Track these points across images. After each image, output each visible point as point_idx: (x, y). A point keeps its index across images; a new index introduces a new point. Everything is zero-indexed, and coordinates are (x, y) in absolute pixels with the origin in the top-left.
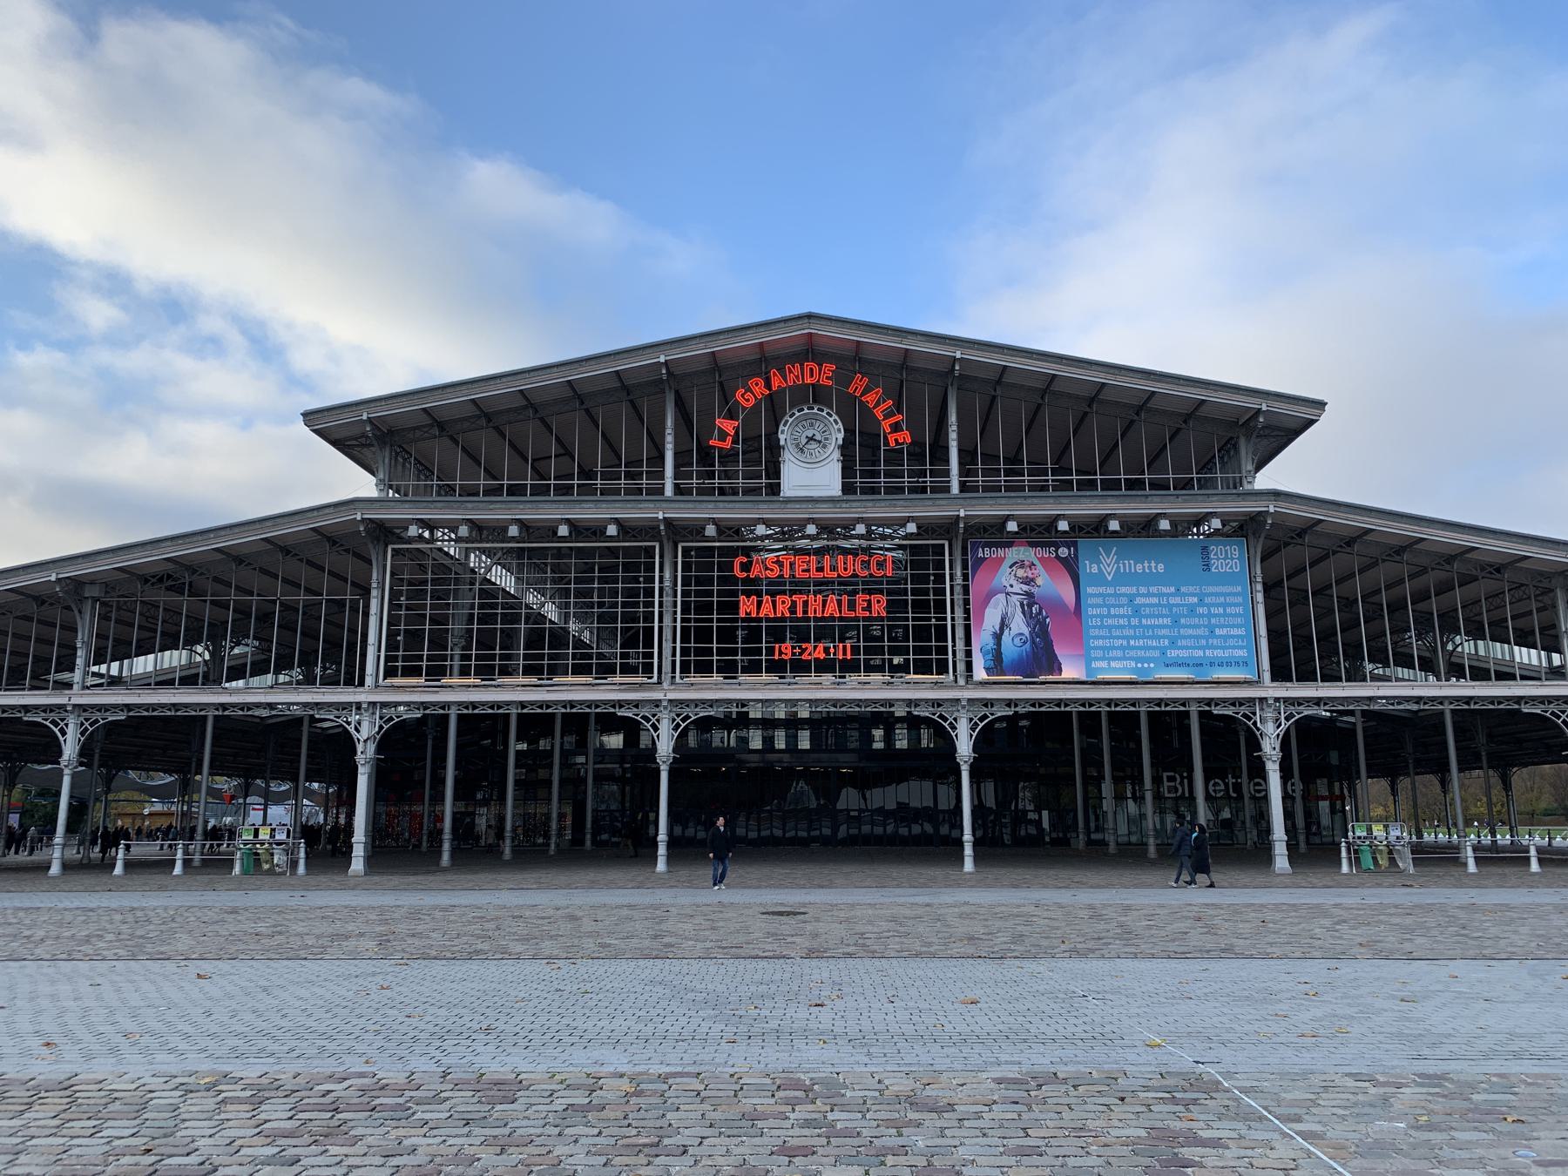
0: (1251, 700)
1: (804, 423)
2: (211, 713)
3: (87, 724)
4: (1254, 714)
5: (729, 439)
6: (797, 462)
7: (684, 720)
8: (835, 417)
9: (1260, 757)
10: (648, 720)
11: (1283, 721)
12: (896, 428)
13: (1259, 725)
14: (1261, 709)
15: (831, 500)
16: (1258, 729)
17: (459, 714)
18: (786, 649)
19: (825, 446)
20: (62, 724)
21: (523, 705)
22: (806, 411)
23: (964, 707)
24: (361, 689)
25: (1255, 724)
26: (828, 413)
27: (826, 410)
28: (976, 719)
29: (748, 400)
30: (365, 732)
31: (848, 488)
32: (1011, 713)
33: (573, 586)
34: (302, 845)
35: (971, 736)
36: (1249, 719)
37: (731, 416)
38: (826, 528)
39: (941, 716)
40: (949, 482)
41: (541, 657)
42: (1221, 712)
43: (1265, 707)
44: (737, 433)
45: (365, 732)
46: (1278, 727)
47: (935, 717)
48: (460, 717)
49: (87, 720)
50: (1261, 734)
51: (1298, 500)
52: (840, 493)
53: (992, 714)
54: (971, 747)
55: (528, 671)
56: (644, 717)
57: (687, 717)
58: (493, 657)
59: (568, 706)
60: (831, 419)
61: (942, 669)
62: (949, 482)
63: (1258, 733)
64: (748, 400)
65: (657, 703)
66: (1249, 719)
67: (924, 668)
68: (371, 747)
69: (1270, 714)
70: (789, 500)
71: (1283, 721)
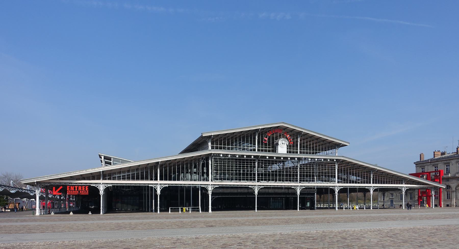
3: (161, 187)
10: (254, 188)
20: (156, 187)
21: (317, 186)
30: (210, 189)
38: (284, 158)
39: (295, 188)
41: (266, 178)
45: (210, 189)
49: (161, 186)
55: (220, 179)
56: (253, 187)
57: (259, 188)
58: (245, 177)
68: (211, 192)
69: (337, 188)
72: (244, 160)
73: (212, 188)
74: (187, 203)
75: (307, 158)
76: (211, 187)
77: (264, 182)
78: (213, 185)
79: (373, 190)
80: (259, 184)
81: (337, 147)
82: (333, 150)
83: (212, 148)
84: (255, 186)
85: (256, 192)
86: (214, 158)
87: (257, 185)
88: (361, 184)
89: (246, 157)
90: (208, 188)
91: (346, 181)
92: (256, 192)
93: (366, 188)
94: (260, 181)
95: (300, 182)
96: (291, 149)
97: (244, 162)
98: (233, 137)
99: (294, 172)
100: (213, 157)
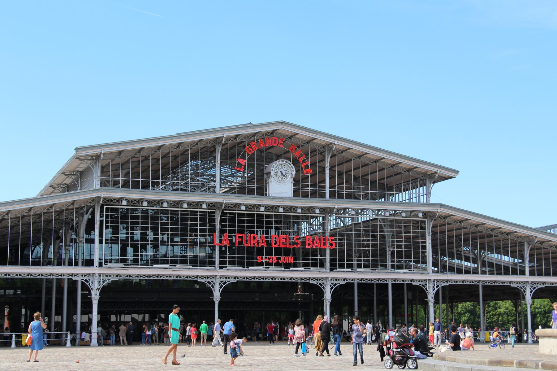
0: (426, 280)
1: (279, 166)
2: (66, 277)
4: (426, 285)
5: (243, 167)
6: (276, 182)
7: (224, 284)
8: (292, 165)
9: (427, 301)
11: (436, 288)
12: (307, 167)
13: (428, 289)
14: (429, 283)
15: (289, 198)
16: (427, 291)
17: (392, 283)
18: (274, 259)
19: (286, 176)
22: (284, 162)
23: (329, 281)
24: (91, 268)
25: (426, 289)
26: (289, 164)
27: (288, 162)
28: (332, 285)
29: (250, 151)
31: (296, 194)
32: (345, 283)
33: (179, 227)
34: (69, 334)
35: (331, 292)
36: (424, 287)
37: (243, 157)
39: (320, 284)
40: (325, 190)
42: (415, 284)
43: (430, 282)
44: (245, 165)
46: (434, 290)
47: (318, 284)
48: (359, 284)
50: (428, 293)
51: (448, 208)
52: (292, 196)
53: (228, 282)
54: (331, 296)
59: (7, 275)
60: (290, 166)
61: (322, 265)
62: (325, 190)
63: (427, 292)
64: (250, 151)
65: (214, 277)
66: (424, 287)
67: (314, 265)
68: (98, 293)
70: (274, 198)
71: (436, 288)
72: (184, 213)
73: (101, 283)
74: (60, 321)
75: (365, 210)
76: (99, 282)
77: (236, 267)
78: (103, 274)
79: (534, 291)
80: (224, 273)
81: (428, 182)
82: (411, 191)
83: (104, 184)
84: (213, 280)
85: (217, 296)
86: (106, 208)
87: (218, 277)
88: (546, 277)
89: (167, 206)
90: (89, 284)
91: (444, 269)
92: (217, 296)
93: (512, 285)
94: (226, 267)
95: (331, 270)
96: (316, 186)
97: (253, 222)
98: (149, 156)
99: (406, 247)
100: (105, 207)
